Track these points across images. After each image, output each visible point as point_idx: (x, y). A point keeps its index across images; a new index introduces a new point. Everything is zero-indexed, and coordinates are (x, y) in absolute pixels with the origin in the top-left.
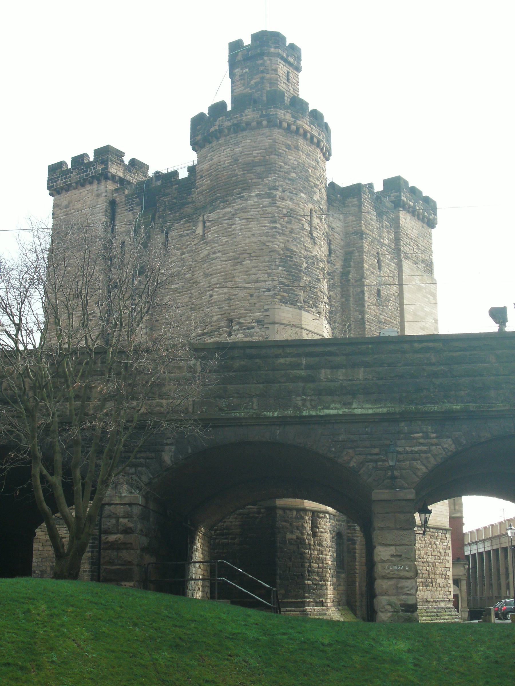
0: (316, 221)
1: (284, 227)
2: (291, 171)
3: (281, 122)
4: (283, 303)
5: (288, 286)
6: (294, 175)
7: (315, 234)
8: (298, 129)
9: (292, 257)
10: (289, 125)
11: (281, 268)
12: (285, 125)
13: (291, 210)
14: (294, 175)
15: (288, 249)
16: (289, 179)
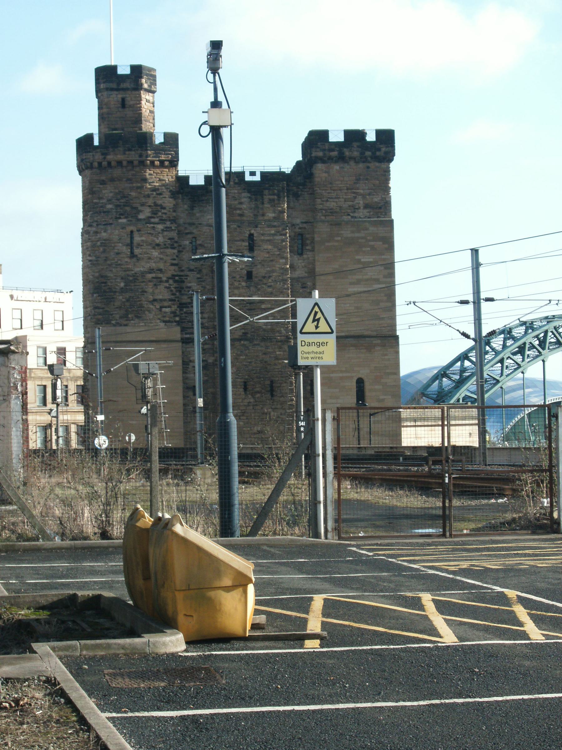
0: (137, 239)
1: (98, 257)
2: (106, 204)
3: (92, 164)
4: (99, 324)
5: (103, 308)
6: (109, 206)
7: (137, 251)
8: (109, 163)
9: (105, 283)
10: (100, 164)
11: (95, 295)
12: (96, 164)
13: (105, 240)
14: (109, 206)
15: (102, 276)
16: (104, 212)
